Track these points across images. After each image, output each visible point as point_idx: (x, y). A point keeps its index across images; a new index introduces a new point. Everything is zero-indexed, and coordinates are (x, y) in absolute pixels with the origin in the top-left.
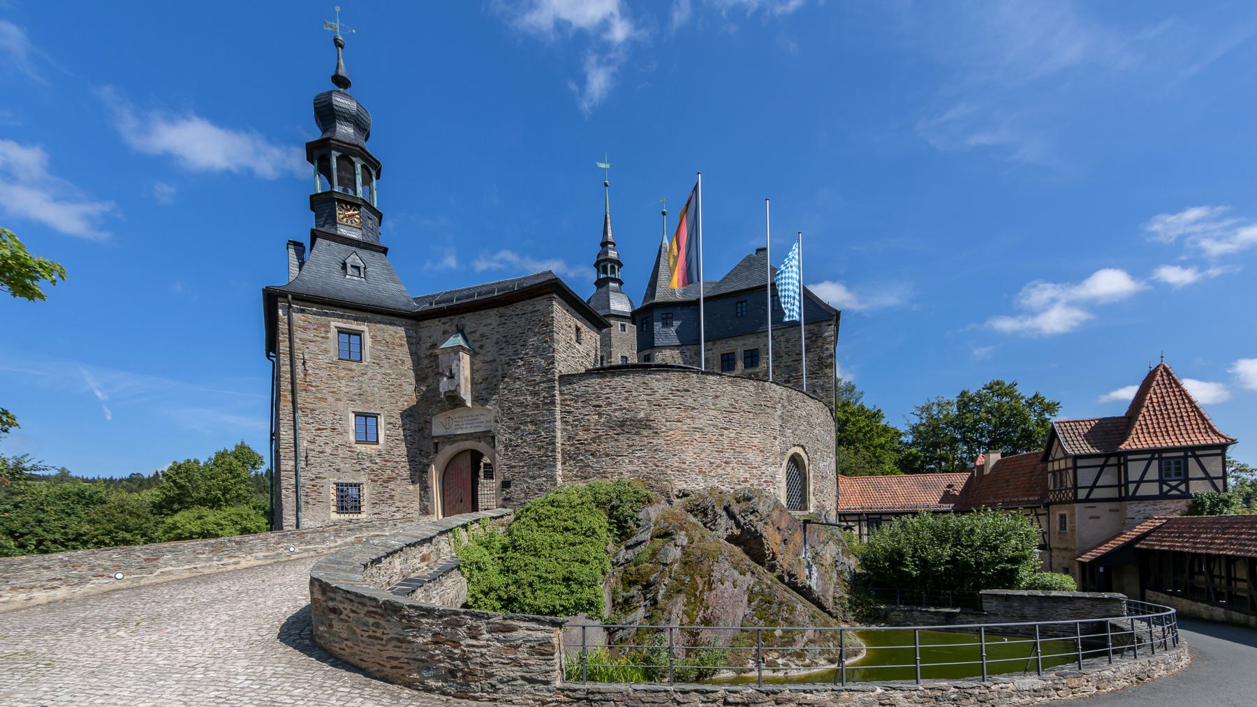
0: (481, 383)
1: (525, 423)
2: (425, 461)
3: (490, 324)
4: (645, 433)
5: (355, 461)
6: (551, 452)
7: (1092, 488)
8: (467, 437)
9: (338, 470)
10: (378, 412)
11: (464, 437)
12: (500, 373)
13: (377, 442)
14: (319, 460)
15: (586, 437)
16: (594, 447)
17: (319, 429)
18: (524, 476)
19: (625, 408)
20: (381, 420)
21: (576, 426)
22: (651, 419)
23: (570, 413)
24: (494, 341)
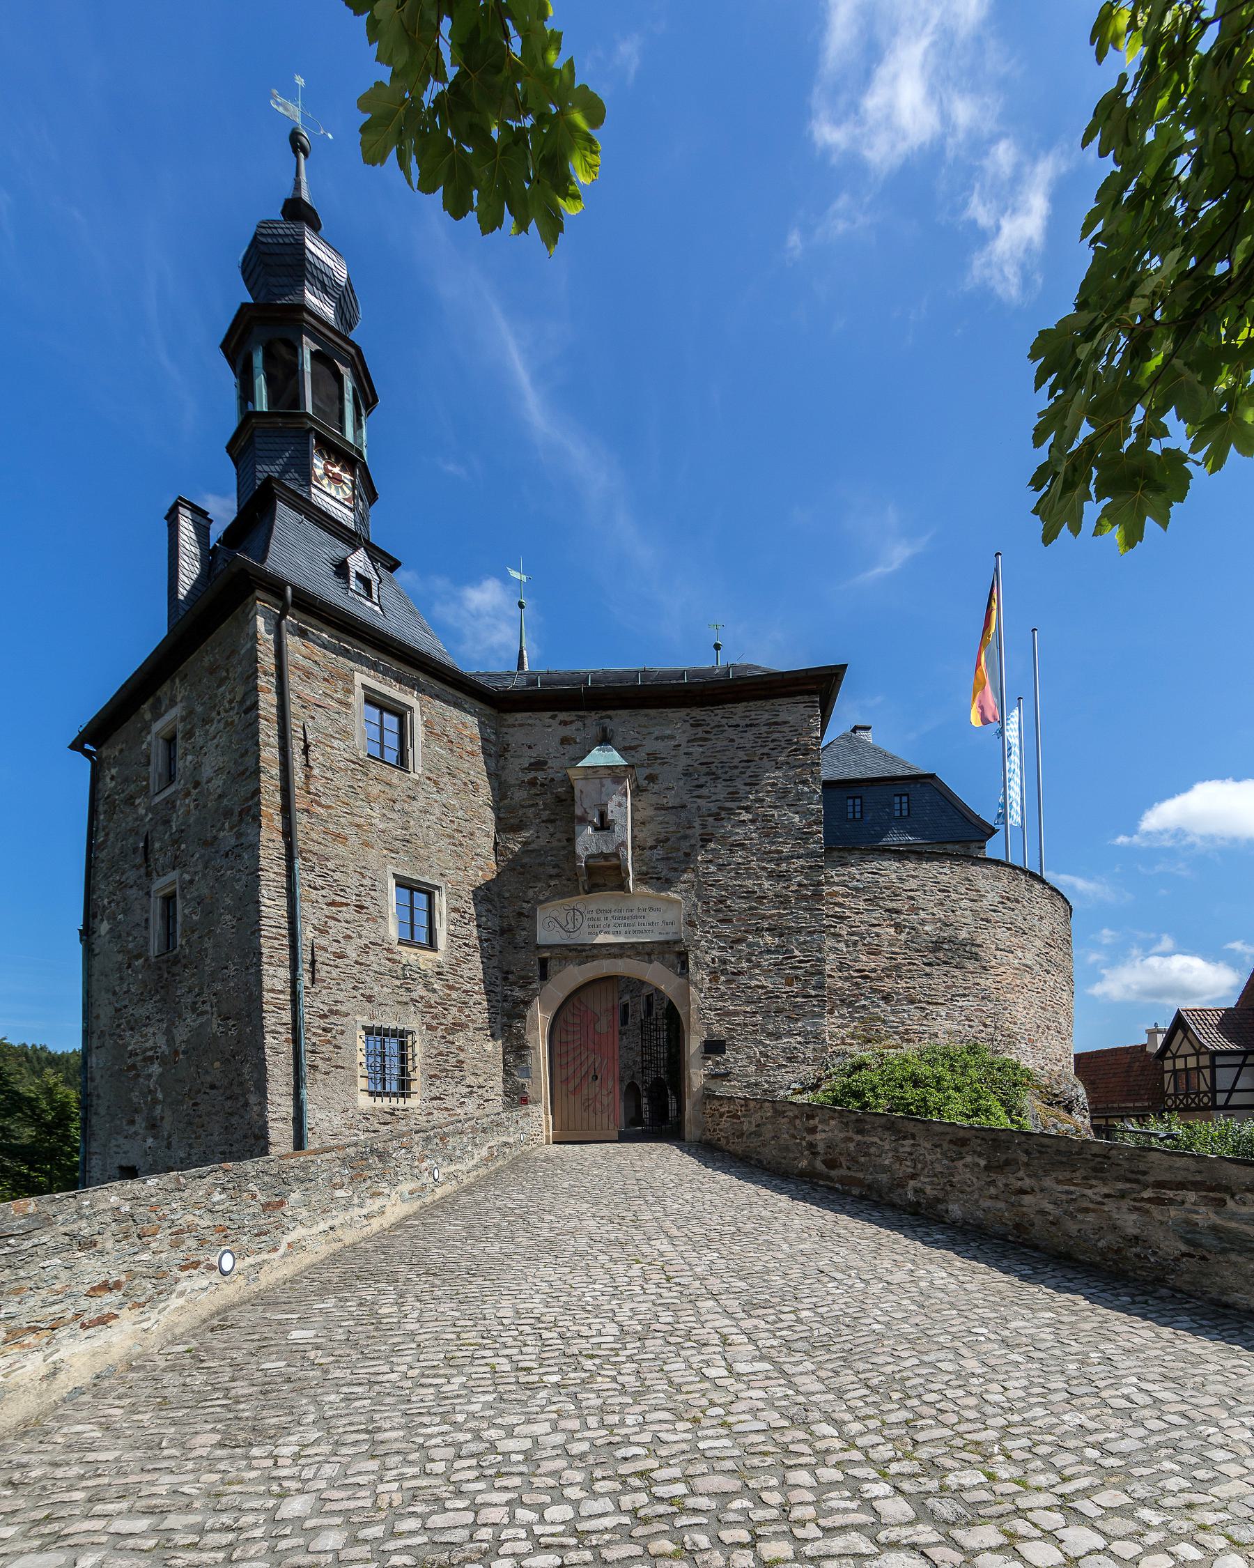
0: (655, 847)
1: (758, 931)
2: (518, 994)
3: (672, 737)
4: (970, 965)
5: (398, 982)
6: (815, 988)
7: (1231, 1091)
8: (619, 951)
9: (369, 999)
10: (436, 883)
11: (615, 951)
12: (697, 830)
13: (432, 945)
14: (334, 974)
15: (873, 965)
16: (888, 984)
17: (333, 904)
18: (755, 1032)
19: (940, 920)
20: (441, 902)
21: (855, 943)
22: (978, 942)
23: (843, 918)
24: (680, 769)
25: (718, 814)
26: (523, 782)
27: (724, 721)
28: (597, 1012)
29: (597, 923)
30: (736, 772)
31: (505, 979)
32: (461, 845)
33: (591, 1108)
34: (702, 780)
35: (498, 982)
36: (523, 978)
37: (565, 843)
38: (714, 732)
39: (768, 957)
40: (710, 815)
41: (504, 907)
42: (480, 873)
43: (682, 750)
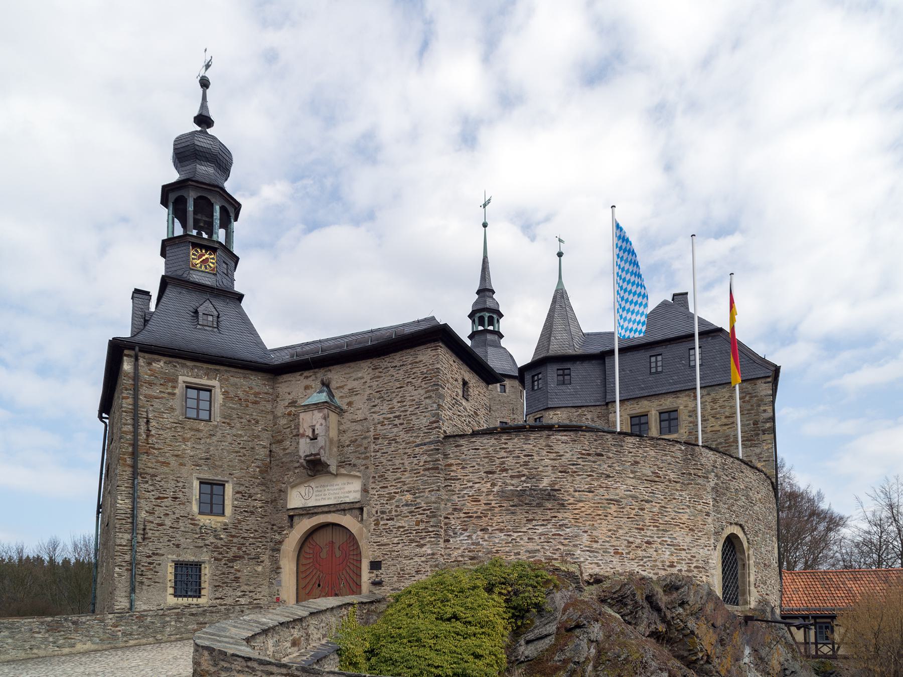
25: (383, 422)
26: (285, 414)
27: (389, 365)
29: (320, 493)
31: (272, 529)
34: (376, 403)
35: (268, 531)
36: (280, 528)
38: (384, 371)
39: (406, 508)
40: (379, 423)
42: (258, 470)
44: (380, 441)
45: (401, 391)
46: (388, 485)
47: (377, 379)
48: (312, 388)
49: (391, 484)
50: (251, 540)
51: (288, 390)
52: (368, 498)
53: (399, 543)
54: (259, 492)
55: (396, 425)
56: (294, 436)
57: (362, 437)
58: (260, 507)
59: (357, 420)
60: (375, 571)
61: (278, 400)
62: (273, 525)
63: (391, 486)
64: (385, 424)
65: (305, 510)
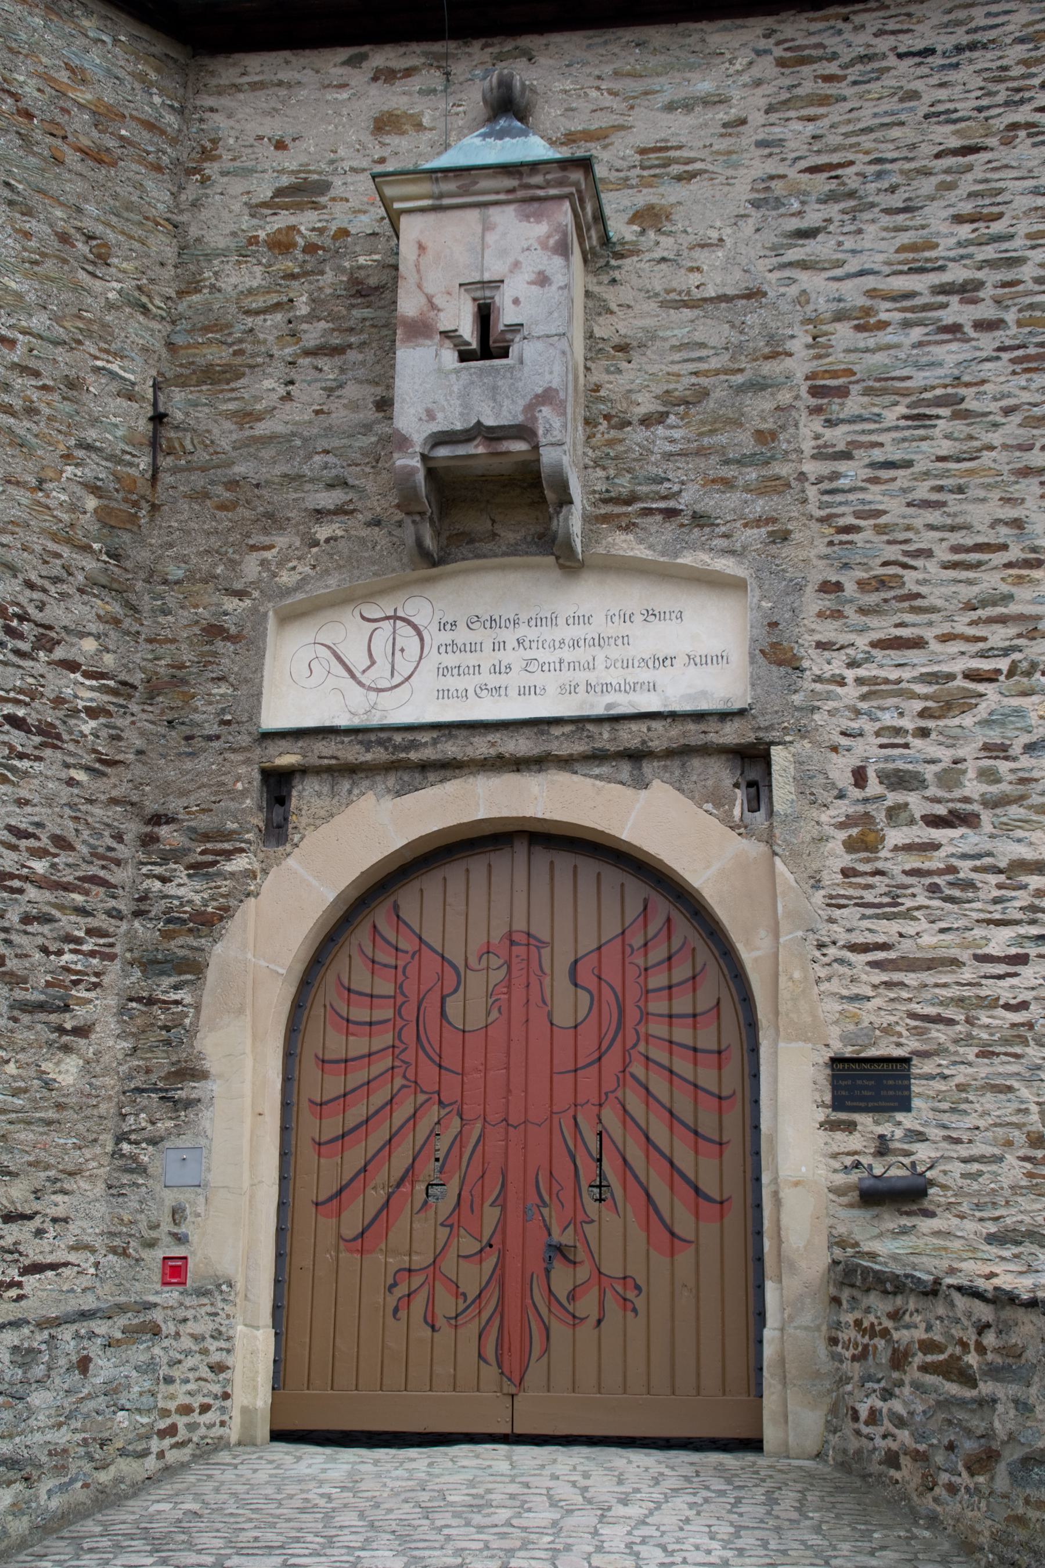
0: (660, 418)
24: (742, 190)
25: (868, 311)
26: (253, 240)
27: (883, 44)
28: (456, 955)
30: (927, 186)
31: (148, 841)
32: (31, 411)
33: (419, 1303)
34: (813, 218)
35: (122, 851)
36: (206, 837)
37: (370, 414)
38: (853, 74)
40: (839, 317)
41: (165, 612)
42: (91, 503)
43: (749, 135)
44: (854, 404)
45: (969, 168)
46: (929, 634)
47: (811, 111)
48: (419, 127)
49: (946, 628)
50: (32, 892)
51: (272, 127)
52: (797, 699)
53: (1022, 960)
54: (93, 627)
55: (955, 329)
56: (307, 353)
57: (739, 379)
58: (93, 713)
59: (697, 294)
60: (864, 1120)
61: (211, 169)
62: (157, 819)
63: (945, 638)
64: (883, 325)
65: (380, 743)
